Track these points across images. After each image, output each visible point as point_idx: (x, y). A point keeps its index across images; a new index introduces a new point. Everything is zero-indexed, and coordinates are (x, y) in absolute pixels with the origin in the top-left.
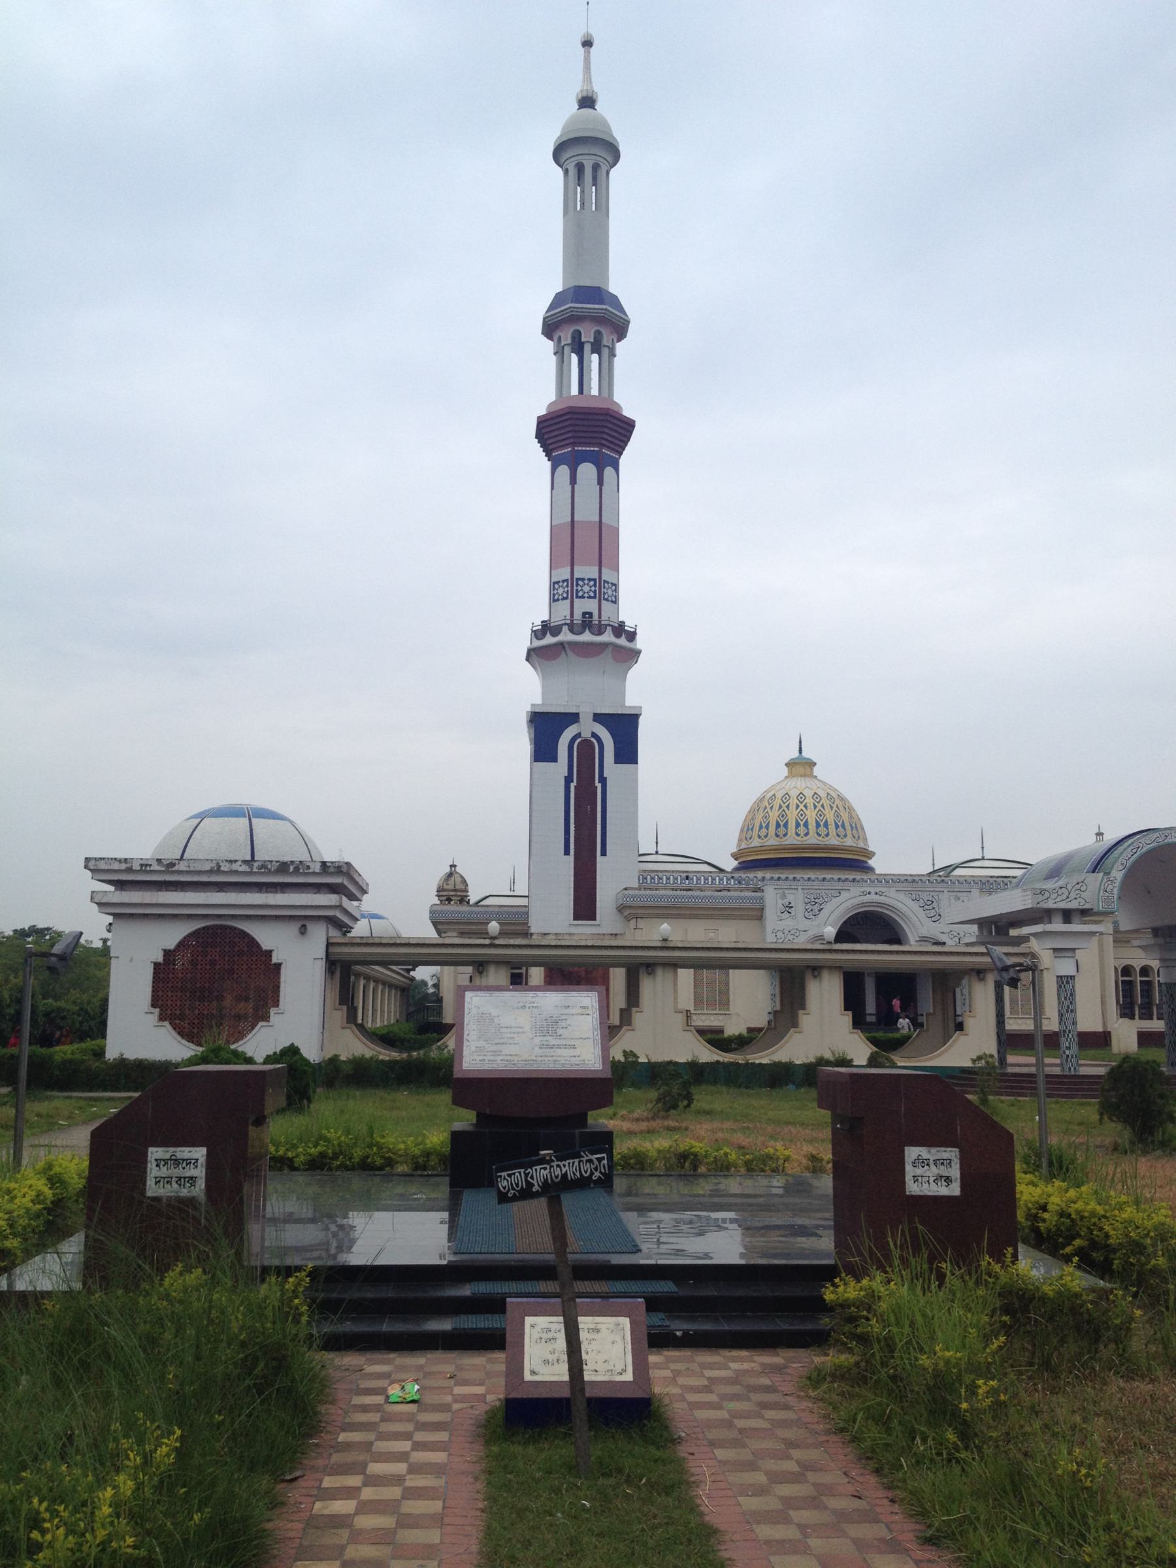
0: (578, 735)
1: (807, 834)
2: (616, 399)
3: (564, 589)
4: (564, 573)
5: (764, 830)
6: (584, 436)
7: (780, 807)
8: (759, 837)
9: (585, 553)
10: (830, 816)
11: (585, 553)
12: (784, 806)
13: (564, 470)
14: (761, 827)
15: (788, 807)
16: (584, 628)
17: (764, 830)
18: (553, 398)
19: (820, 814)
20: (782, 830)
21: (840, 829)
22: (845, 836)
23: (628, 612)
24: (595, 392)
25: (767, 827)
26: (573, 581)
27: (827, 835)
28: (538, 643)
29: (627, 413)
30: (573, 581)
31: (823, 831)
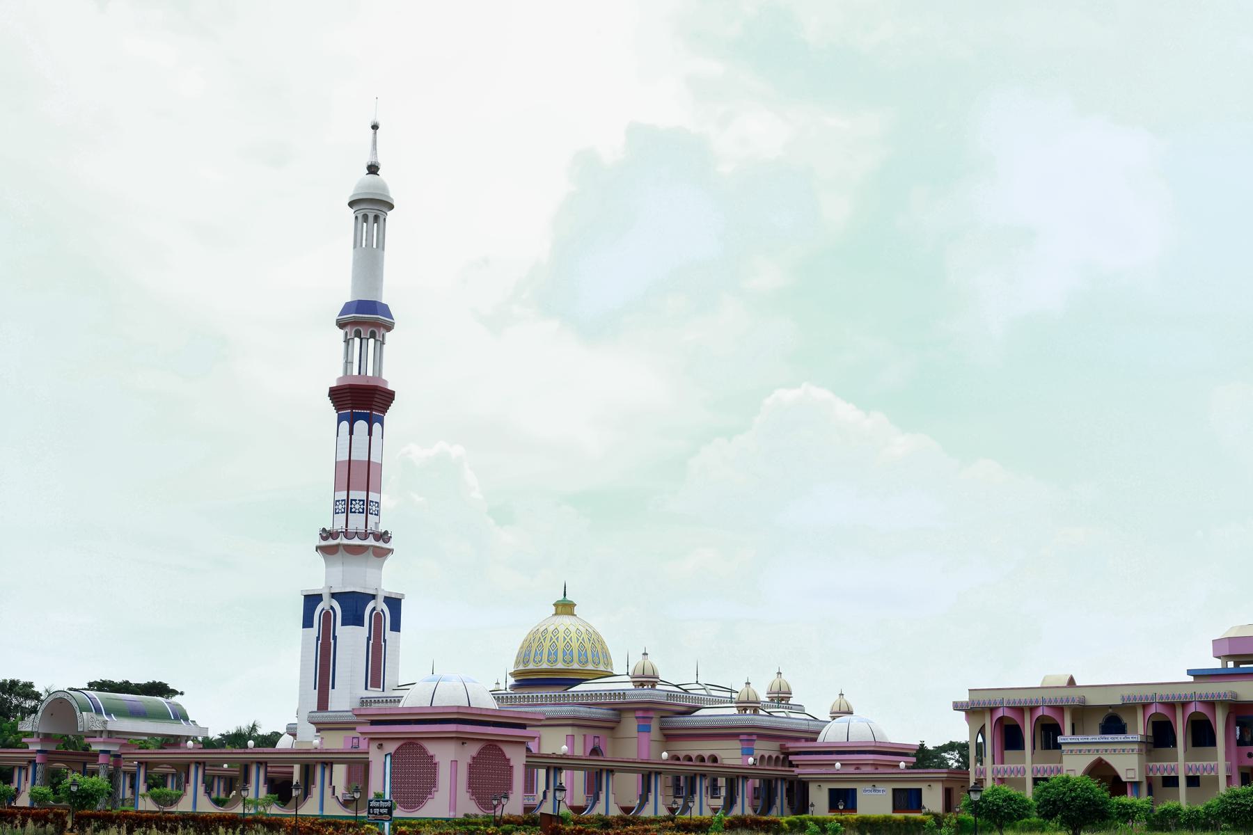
0: (374, 609)
2: (384, 377)
3: (347, 507)
4: (342, 495)
6: (361, 401)
9: (358, 478)
11: (358, 478)
13: (345, 425)
16: (355, 536)
18: (341, 375)
23: (383, 524)
24: (370, 373)
26: (348, 502)
28: (324, 543)
29: (390, 387)
30: (348, 502)
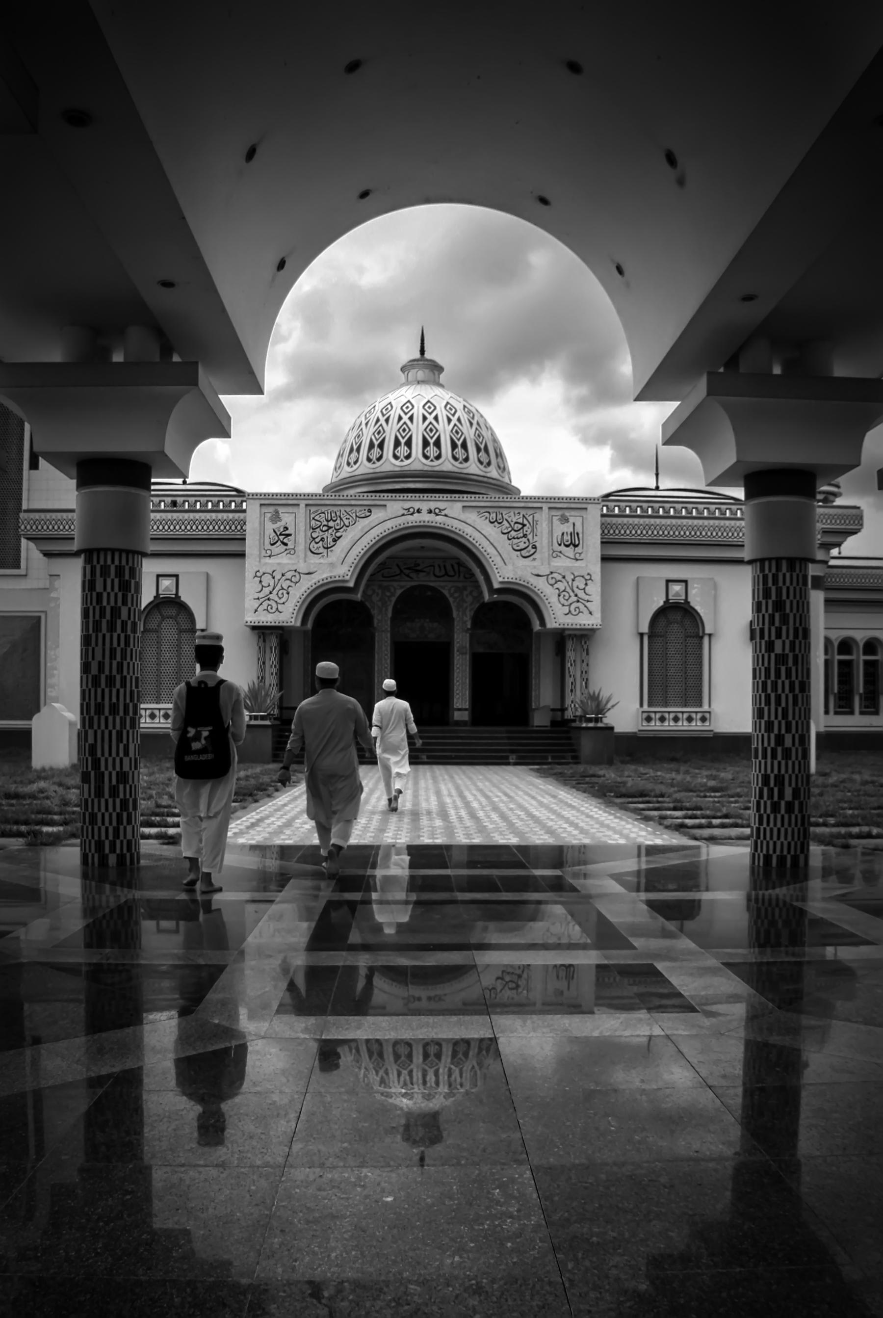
1: (438, 457)
5: (376, 452)
7: (400, 418)
8: (369, 460)
10: (469, 433)
12: (405, 418)
14: (371, 446)
15: (411, 418)
17: (376, 452)
19: (431, 429)
20: (403, 450)
21: (482, 453)
22: (489, 464)
25: (381, 446)
27: (466, 460)
31: (460, 452)
